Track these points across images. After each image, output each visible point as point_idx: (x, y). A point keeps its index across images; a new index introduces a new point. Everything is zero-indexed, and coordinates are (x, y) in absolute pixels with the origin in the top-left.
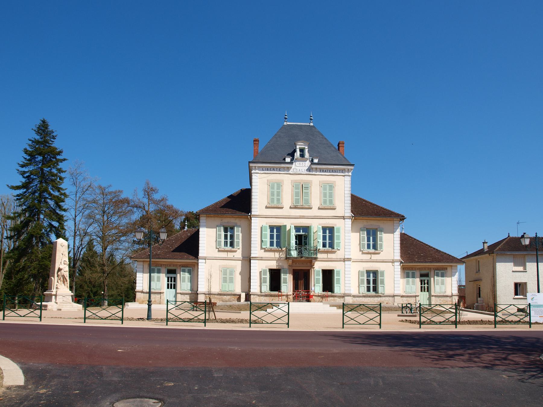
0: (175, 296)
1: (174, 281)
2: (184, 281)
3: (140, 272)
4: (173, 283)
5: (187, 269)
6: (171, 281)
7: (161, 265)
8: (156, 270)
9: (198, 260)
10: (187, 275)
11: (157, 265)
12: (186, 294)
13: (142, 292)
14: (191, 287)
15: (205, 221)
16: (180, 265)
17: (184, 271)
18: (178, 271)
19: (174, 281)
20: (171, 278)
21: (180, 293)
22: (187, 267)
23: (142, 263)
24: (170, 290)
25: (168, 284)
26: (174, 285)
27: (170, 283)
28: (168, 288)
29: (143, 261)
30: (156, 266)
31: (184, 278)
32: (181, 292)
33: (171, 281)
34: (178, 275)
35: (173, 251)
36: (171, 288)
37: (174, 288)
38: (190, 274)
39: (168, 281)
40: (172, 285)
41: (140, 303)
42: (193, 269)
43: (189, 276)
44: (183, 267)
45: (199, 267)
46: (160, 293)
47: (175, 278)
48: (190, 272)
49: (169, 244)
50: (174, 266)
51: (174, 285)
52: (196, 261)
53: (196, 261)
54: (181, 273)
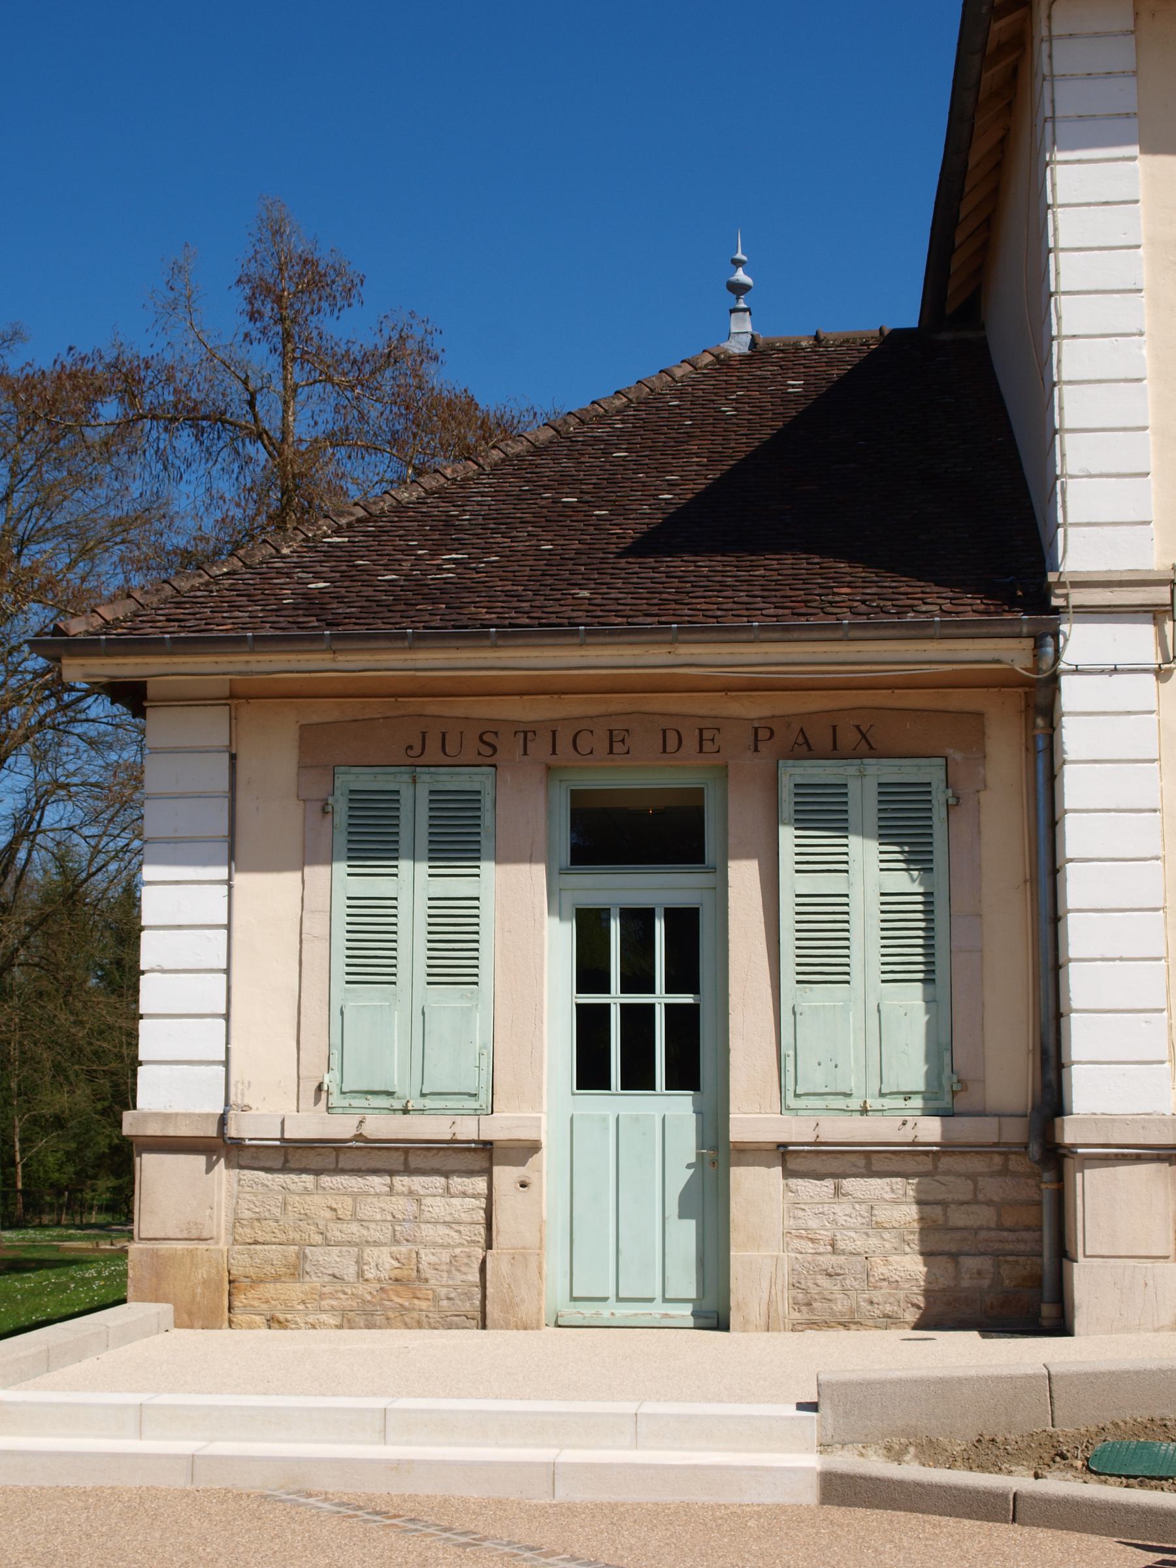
0: (707, 1200)
1: (684, 975)
2: (827, 965)
3: (183, 848)
4: (660, 999)
5: (863, 781)
6: (637, 979)
7: (488, 745)
8: (416, 816)
9: (1045, 637)
10: (869, 875)
11: (427, 731)
12: (869, 1160)
13: (220, 1146)
14: (942, 1047)
15: (1121, 54)
16: (761, 734)
17: (825, 813)
18: (732, 811)
19: (684, 975)
20: (638, 922)
21: (784, 1156)
22: (868, 748)
23: (211, 726)
24: (616, 1104)
25: (590, 1022)
26: (684, 1022)
27: (615, 999)
28: (591, 1075)
29: (236, 697)
30: (415, 759)
31: (828, 919)
32: (795, 1129)
33: (637, 979)
34: (743, 876)
35: (651, 544)
36: (638, 1077)
37: (684, 1075)
38: (918, 858)
39: (590, 976)
40: (648, 1025)
41: (191, 1316)
42: (977, 793)
43: (904, 882)
44: (804, 748)
45: (1074, 736)
46: (484, 1155)
47: (685, 925)
48: (907, 829)
49: (563, 481)
50: (669, 739)
51: (684, 1022)
52: (1013, 654)
53: (1013, 654)
54: (787, 835)
